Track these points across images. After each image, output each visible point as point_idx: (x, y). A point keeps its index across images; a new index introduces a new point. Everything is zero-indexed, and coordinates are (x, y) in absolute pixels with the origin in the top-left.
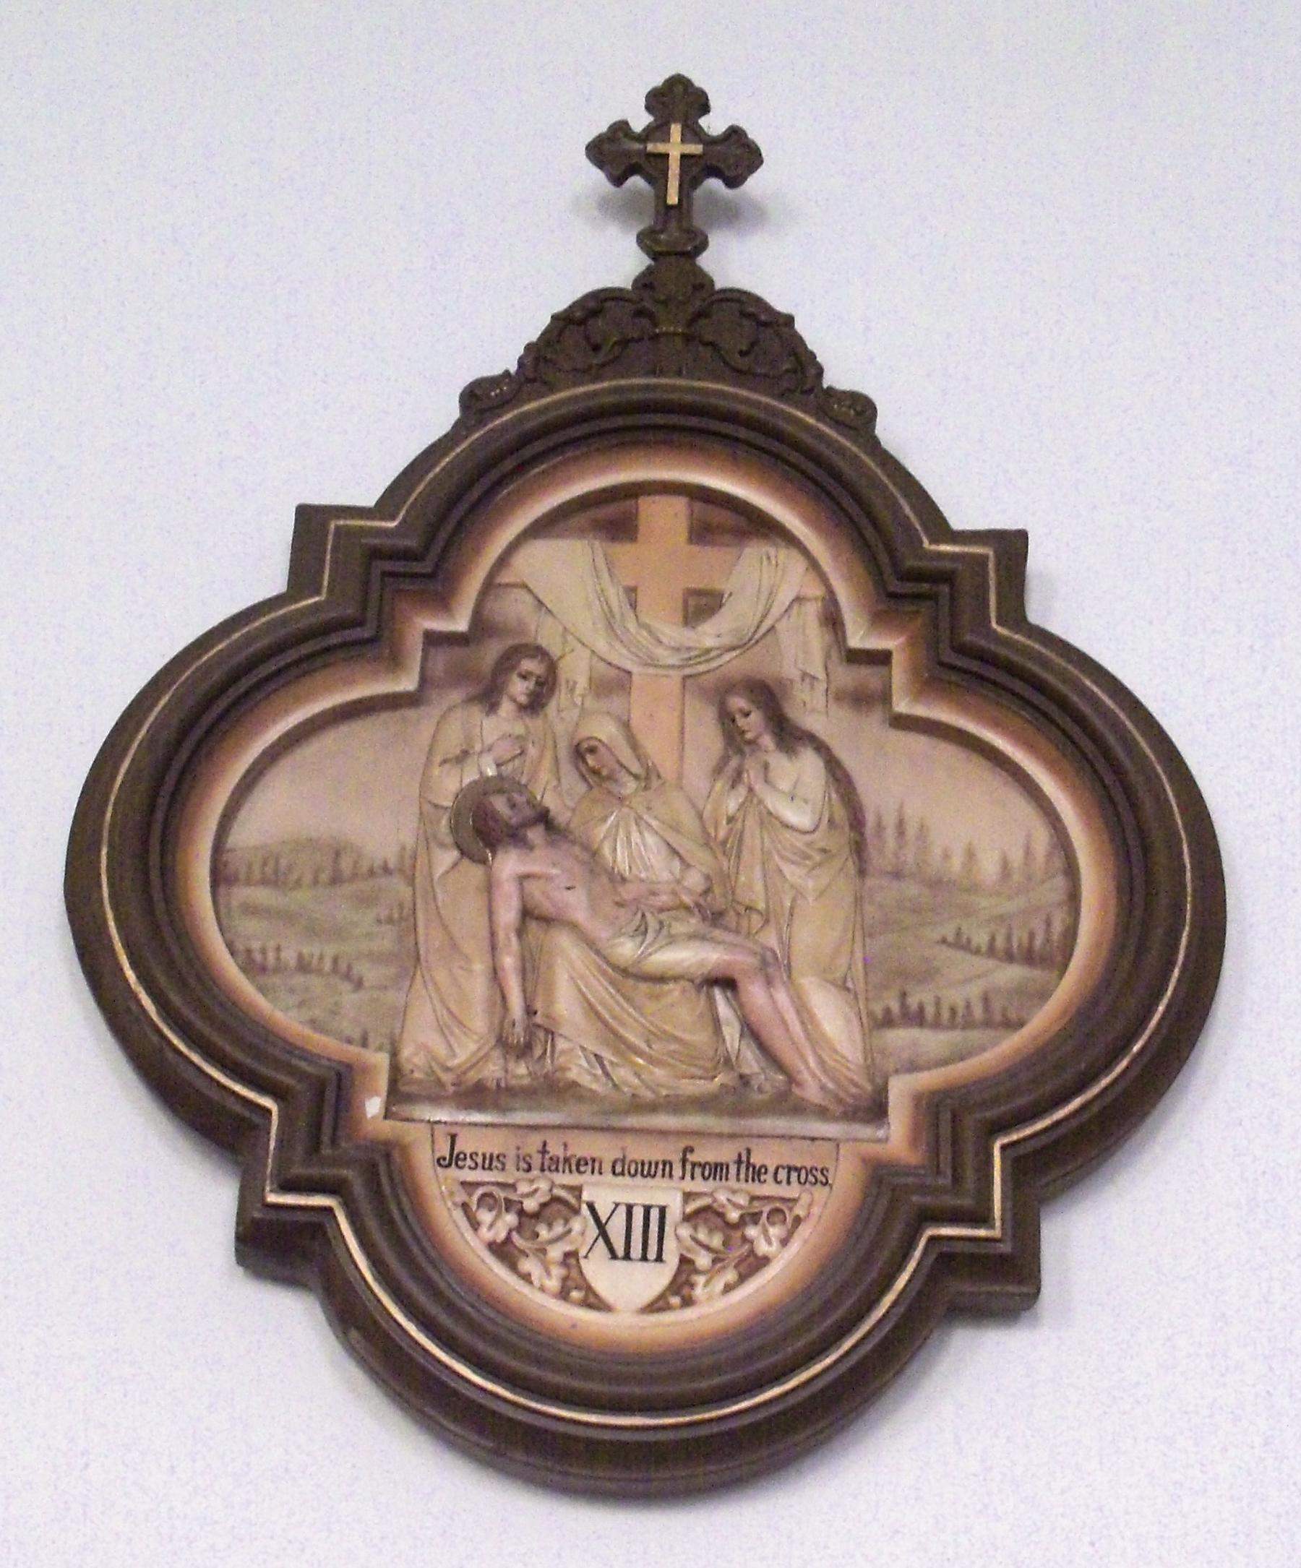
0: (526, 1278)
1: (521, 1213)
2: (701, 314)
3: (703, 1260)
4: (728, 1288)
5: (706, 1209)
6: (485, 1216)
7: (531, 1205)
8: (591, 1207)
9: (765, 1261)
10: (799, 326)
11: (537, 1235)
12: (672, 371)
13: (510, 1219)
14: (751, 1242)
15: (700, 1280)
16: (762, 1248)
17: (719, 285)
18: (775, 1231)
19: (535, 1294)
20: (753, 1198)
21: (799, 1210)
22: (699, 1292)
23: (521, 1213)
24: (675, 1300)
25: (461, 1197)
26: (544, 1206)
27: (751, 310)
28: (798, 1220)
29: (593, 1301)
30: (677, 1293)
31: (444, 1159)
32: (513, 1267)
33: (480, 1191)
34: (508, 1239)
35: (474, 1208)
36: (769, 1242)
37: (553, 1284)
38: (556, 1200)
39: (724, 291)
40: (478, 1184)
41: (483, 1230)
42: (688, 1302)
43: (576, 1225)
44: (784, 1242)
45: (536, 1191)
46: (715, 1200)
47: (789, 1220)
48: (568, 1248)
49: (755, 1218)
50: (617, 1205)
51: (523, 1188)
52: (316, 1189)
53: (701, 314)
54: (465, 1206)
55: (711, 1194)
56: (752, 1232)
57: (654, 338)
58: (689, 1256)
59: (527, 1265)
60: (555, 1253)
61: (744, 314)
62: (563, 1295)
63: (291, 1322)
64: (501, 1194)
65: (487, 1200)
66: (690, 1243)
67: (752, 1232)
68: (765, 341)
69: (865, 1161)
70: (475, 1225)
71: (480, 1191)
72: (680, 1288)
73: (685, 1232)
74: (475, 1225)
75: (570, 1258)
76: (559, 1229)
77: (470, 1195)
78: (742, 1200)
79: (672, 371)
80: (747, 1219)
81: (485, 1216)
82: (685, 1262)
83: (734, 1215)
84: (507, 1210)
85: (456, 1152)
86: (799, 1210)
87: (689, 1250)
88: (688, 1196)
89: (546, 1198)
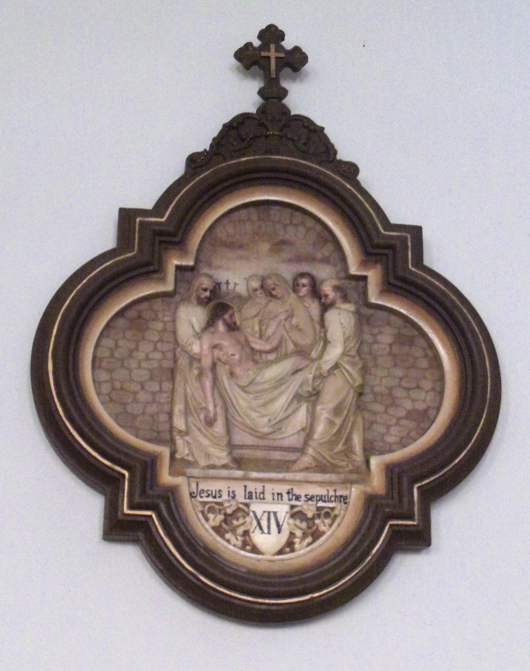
0: (228, 541)
1: (225, 514)
2: (285, 126)
3: (299, 533)
4: (309, 544)
5: (300, 512)
6: (211, 516)
7: (229, 511)
8: (254, 512)
9: (323, 533)
10: (326, 131)
11: (232, 523)
12: (270, 154)
13: (221, 517)
14: (318, 526)
15: (297, 540)
16: (322, 528)
17: (293, 113)
18: (328, 521)
19: (229, 548)
20: (319, 509)
21: (336, 512)
22: (297, 546)
23: (225, 514)
24: (288, 549)
25: (200, 508)
26: (234, 512)
27: (306, 124)
28: (336, 516)
29: (255, 550)
30: (288, 547)
31: (194, 493)
32: (223, 537)
33: (207, 506)
34: (220, 526)
35: (206, 512)
36: (325, 525)
37: (239, 543)
38: (239, 509)
39: (296, 115)
40: (207, 503)
41: (211, 521)
42: (293, 550)
43: (248, 519)
44: (331, 526)
45: (231, 505)
46: (303, 508)
47: (332, 516)
48: (246, 529)
49: (319, 516)
50: (264, 512)
51: (226, 504)
52: (139, 506)
53: (285, 126)
54: (203, 512)
55: (301, 506)
56: (317, 521)
57: (267, 136)
58: (293, 532)
59: (228, 536)
60: (240, 531)
61: (304, 127)
62: (243, 548)
63: (130, 559)
64: (217, 507)
65: (211, 510)
66: (293, 527)
67: (317, 521)
68: (311, 137)
69: (365, 493)
70: (207, 519)
71: (207, 506)
72: (290, 545)
73: (291, 521)
74: (207, 519)
75: (246, 533)
76: (241, 521)
77: (204, 507)
78: (313, 509)
79: (270, 154)
80: (316, 516)
81: (211, 516)
82: (292, 534)
83: (310, 515)
84: (220, 513)
85: (199, 490)
86: (336, 512)
87: (293, 530)
88: (292, 507)
89: (234, 508)
